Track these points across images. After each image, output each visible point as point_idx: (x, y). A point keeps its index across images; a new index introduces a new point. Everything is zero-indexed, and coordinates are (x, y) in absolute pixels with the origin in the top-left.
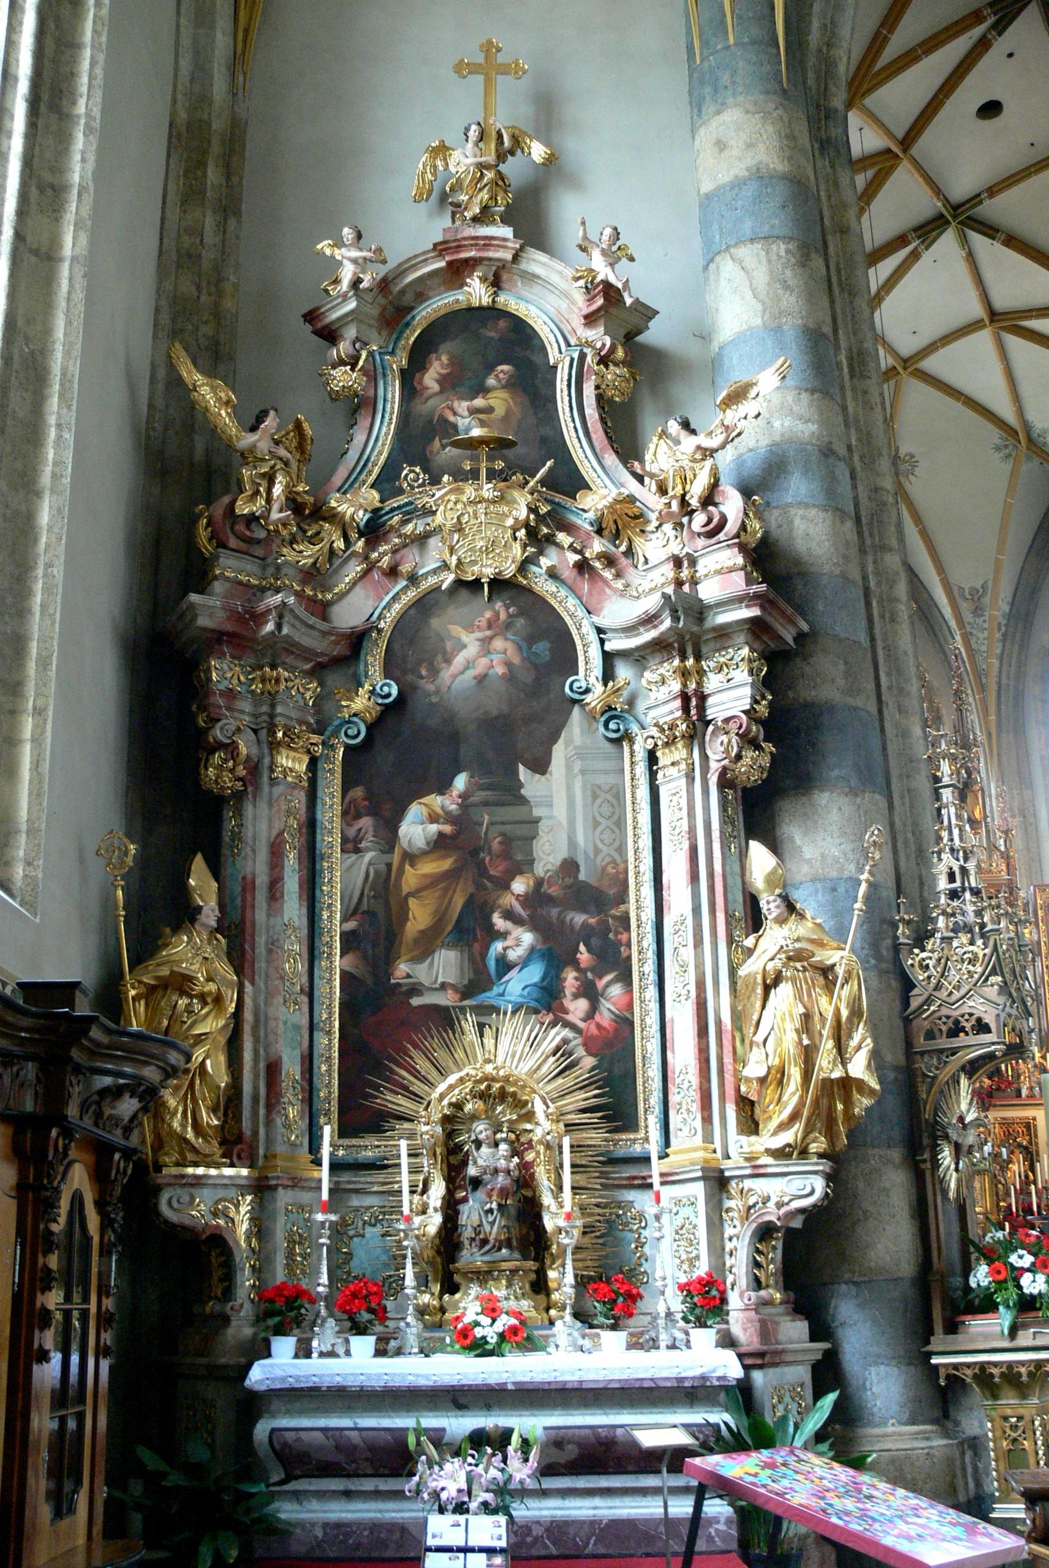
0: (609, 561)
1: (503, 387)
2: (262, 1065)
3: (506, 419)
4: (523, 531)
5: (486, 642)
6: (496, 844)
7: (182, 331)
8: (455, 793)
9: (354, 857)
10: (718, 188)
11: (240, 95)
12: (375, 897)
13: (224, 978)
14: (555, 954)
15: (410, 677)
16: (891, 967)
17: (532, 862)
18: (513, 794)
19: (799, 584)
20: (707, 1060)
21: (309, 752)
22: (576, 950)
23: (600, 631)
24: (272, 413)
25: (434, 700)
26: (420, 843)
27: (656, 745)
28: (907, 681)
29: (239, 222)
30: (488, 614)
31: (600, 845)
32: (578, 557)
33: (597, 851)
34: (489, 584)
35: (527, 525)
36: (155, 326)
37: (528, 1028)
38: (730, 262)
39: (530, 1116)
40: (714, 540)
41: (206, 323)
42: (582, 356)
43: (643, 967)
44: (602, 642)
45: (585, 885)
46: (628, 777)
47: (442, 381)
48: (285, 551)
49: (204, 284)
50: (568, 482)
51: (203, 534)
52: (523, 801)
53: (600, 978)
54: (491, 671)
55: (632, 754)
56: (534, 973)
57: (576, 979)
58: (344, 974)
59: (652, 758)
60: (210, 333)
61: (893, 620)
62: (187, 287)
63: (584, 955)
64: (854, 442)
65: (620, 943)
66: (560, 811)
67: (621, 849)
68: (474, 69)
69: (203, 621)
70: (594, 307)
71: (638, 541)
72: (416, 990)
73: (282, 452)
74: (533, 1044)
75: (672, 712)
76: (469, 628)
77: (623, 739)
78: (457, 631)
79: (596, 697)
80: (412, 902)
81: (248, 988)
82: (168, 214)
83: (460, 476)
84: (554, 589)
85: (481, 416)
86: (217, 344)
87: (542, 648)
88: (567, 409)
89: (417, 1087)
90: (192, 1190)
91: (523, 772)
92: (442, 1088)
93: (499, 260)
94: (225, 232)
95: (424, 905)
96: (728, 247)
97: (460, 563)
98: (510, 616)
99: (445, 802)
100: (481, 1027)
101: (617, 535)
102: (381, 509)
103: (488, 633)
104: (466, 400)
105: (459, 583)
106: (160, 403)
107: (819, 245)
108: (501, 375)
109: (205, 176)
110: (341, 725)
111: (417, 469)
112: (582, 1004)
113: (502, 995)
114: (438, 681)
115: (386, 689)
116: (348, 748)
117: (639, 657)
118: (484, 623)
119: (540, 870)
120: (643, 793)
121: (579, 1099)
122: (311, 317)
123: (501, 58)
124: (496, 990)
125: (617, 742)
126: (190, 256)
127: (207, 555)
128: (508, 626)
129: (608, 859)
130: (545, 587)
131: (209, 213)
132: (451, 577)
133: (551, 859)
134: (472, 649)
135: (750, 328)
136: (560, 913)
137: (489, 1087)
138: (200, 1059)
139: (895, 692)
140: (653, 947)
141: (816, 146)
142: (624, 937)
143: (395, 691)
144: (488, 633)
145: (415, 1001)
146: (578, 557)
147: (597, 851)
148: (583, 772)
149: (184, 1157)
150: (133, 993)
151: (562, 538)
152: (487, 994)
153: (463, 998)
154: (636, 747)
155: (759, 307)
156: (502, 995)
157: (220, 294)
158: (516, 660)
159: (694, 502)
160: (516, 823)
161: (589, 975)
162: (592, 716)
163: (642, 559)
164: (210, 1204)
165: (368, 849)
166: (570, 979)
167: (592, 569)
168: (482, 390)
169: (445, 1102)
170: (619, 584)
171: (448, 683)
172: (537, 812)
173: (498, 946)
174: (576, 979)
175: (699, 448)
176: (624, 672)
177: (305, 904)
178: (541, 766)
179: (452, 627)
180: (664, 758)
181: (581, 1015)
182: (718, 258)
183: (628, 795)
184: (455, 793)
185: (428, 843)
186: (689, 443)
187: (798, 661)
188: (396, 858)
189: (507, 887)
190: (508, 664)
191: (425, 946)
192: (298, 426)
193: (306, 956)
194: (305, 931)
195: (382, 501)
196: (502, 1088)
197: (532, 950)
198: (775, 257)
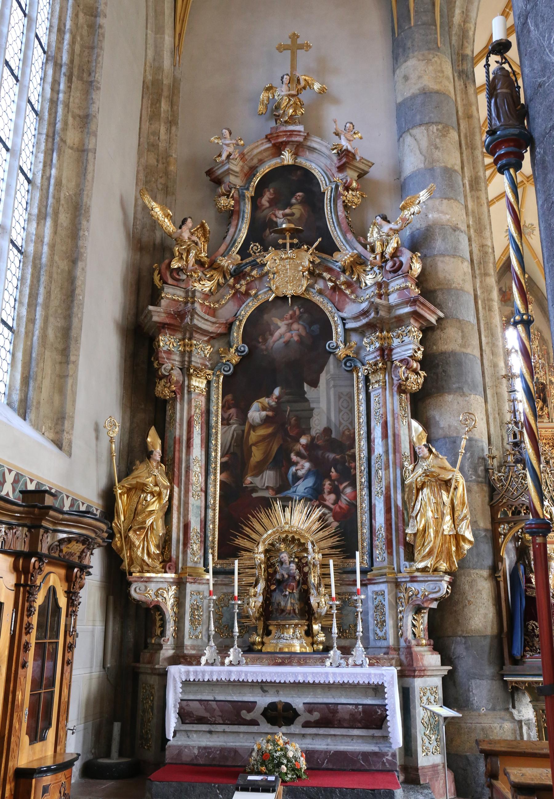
0: (349, 285)
2: (182, 525)
3: (300, 219)
5: (289, 325)
6: (293, 421)
7: (150, 181)
8: (274, 397)
9: (227, 427)
10: (404, 100)
11: (177, 65)
12: (236, 446)
13: (163, 485)
14: (320, 472)
16: (483, 480)
17: (310, 429)
18: (301, 397)
19: (439, 294)
20: (391, 525)
21: (206, 378)
22: (330, 471)
23: (343, 319)
24: (189, 220)
25: (265, 353)
26: (258, 420)
27: (369, 373)
28: (497, 340)
29: (177, 128)
30: (291, 312)
31: (342, 421)
32: (332, 284)
33: (341, 423)
35: (309, 270)
36: (137, 179)
37: (306, 508)
39: (306, 550)
40: (396, 274)
41: (161, 177)
42: (337, 187)
43: (361, 479)
44: (344, 324)
45: (335, 440)
46: (355, 389)
47: (270, 201)
48: (196, 284)
50: (329, 248)
51: (157, 278)
52: (307, 400)
53: (341, 484)
55: (358, 377)
56: (310, 482)
57: (330, 484)
58: (221, 482)
59: (367, 379)
60: (163, 182)
61: (490, 310)
62: (152, 161)
63: (333, 473)
64: (471, 223)
65: (351, 468)
66: (323, 405)
67: (352, 423)
69: (155, 318)
70: (342, 163)
72: (255, 489)
73: (195, 238)
74: (308, 516)
75: (376, 357)
76: (282, 319)
77: (353, 369)
79: (341, 352)
80: (254, 448)
81: (176, 489)
82: (143, 126)
83: (278, 247)
85: (289, 218)
86: (167, 187)
87: (316, 328)
89: (254, 536)
90: (147, 584)
91: (306, 387)
92: (265, 536)
93: (297, 142)
95: (258, 450)
96: (408, 130)
97: (277, 288)
98: (301, 313)
99: (270, 401)
100: (284, 507)
101: (352, 273)
103: (290, 321)
104: (281, 210)
105: (277, 298)
106: (139, 216)
107: (455, 125)
108: (298, 198)
109: (160, 107)
110: (222, 366)
111: (257, 244)
112: (332, 497)
113: (295, 492)
115: (242, 349)
116: (225, 376)
117: (361, 331)
118: (288, 316)
119: (313, 433)
120: (362, 396)
121: (330, 542)
122: (209, 173)
123: (299, 41)
124: (292, 490)
125: (351, 372)
126: (153, 145)
127: (159, 287)
128: (300, 318)
129: (345, 428)
130: (318, 299)
131: (162, 124)
133: (318, 428)
135: (418, 170)
136: (322, 453)
137: (287, 536)
138: (150, 523)
139: (490, 345)
140: (366, 470)
141: (456, 75)
142: (353, 465)
143: (247, 349)
144: (290, 321)
145: (254, 495)
146: (332, 284)
147: (341, 423)
148: (334, 386)
149: (142, 569)
150: (120, 491)
151: (326, 275)
152: (288, 492)
153: (276, 494)
154: (360, 374)
155: (423, 158)
156: (295, 492)
157: (168, 164)
158: (304, 334)
159: (387, 256)
160: (302, 410)
161: (336, 483)
162: (338, 360)
163: (364, 284)
164: (155, 591)
165: (233, 424)
166: (327, 484)
167: (340, 290)
168: (289, 205)
169: (267, 543)
171: (271, 344)
172: (312, 405)
173: (293, 469)
174: (330, 484)
175: (391, 229)
176: (354, 338)
177: (204, 449)
178: (314, 384)
179: (273, 319)
180: (373, 379)
181: (332, 501)
182: (404, 135)
183: (356, 397)
184: (274, 397)
185: (261, 421)
186: (386, 228)
187: (438, 332)
188: (247, 427)
189: (298, 441)
190: (300, 336)
191: (259, 470)
192: (202, 226)
193: (204, 474)
194: (204, 462)
195: (242, 260)
196: (293, 537)
197: (309, 471)
198: (431, 133)
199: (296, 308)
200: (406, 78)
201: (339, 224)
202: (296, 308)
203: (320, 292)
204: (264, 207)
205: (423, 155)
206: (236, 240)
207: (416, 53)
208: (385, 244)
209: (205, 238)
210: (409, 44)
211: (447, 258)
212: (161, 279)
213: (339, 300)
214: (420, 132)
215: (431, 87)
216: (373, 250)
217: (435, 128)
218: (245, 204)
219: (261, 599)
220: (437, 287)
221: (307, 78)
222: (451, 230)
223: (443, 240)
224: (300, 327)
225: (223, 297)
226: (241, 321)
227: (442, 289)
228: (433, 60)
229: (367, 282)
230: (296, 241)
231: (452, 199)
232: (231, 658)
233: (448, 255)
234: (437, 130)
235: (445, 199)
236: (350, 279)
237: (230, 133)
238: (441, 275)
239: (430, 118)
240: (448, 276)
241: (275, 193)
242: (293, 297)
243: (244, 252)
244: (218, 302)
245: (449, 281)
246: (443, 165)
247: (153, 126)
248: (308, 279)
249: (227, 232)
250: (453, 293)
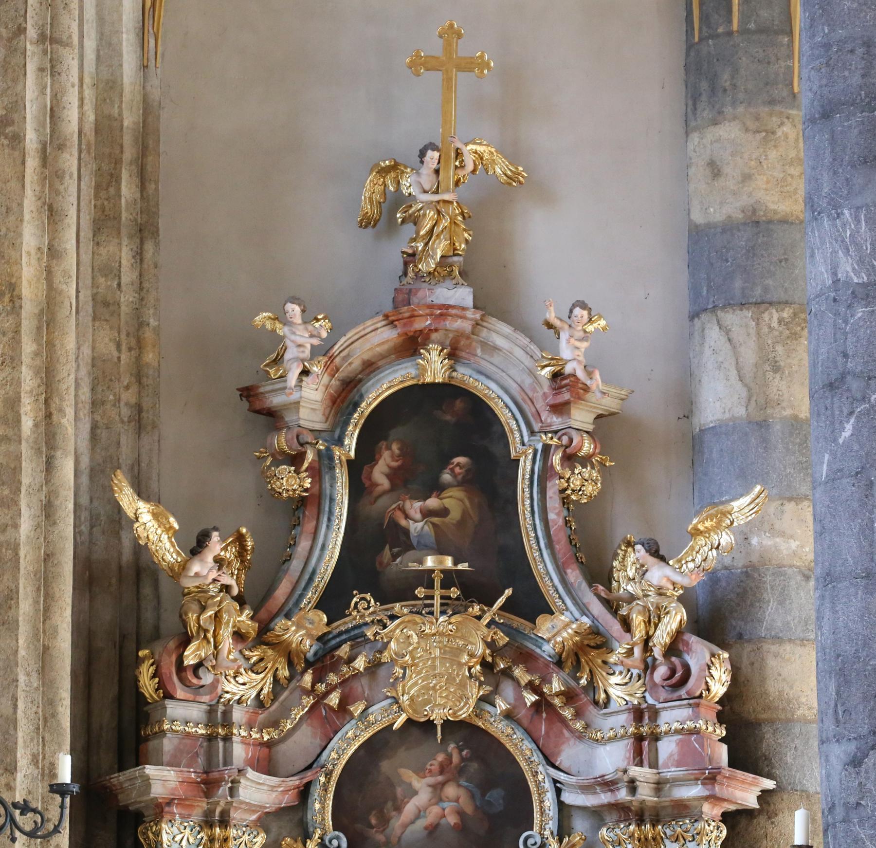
1: (460, 484)
3: (461, 523)
4: (478, 667)
5: (437, 788)
7: (103, 403)
10: (709, 226)
11: (152, 64)
15: (359, 826)
24: (215, 536)
29: (157, 244)
30: (441, 757)
34: (442, 725)
35: (484, 663)
38: (716, 328)
40: (675, 695)
41: (127, 388)
44: (558, 792)
47: (393, 475)
49: (123, 336)
54: (443, 821)
60: (133, 401)
62: (107, 348)
68: (429, 64)
71: (600, 673)
76: (421, 772)
78: (408, 775)
84: (509, 731)
85: (435, 520)
87: (496, 795)
88: (528, 515)
94: (141, 260)
98: (463, 759)
102: (329, 633)
103: (440, 778)
105: (409, 721)
106: (84, 500)
108: (457, 470)
111: (368, 596)
114: (388, 831)
118: (435, 767)
122: (248, 393)
126: (106, 304)
128: (461, 771)
130: (500, 729)
131: (125, 241)
132: (403, 718)
134: (423, 796)
135: (733, 419)
144: (440, 778)
155: (744, 393)
157: (140, 345)
158: (469, 809)
163: (603, 696)
167: (550, 706)
168: (436, 487)
170: (579, 725)
171: (398, 832)
176: (580, 826)
182: (704, 317)
186: (658, 574)
187: (762, 820)
190: (460, 813)
195: (328, 624)
198: (766, 330)
199: (452, 746)
200: (715, 170)
201: (550, 545)
202: (452, 746)
203: (508, 716)
204: (379, 489)
205: (746, 385)
206: (314, 573)
207: (741, 109)
208: (654, 619)
209: (242, 562)
210: (725, 79)
211: (788, 647)
212: (161, 686)
213: (547, 733)
215: (772, 207)
216: (626, 624)
217: (776, 316)
218: (333, 478)
220: (764, 716)
221: (480, 149)
222: (799, 578)
224: (462, 794)
225: (285, 712)
226: (329, 775)
227: (772, 722)
228: (779, 133)
229: (611, 691)
230: (454, 592)
233: (790, 640)
234: (780, 322)
235: (790, 499)
236: (573, 683)
237: (303, 311)
238: (773, 687)
239: (766, 289)
240: (787, 689)
241: (403, 454)
242: (446, 723)
243: (333, 602)
244: (275, 724)
245: (789, 701)
246: (788, 412)
247: (103, 251)
248: (481, 684)
250: (797, 730)
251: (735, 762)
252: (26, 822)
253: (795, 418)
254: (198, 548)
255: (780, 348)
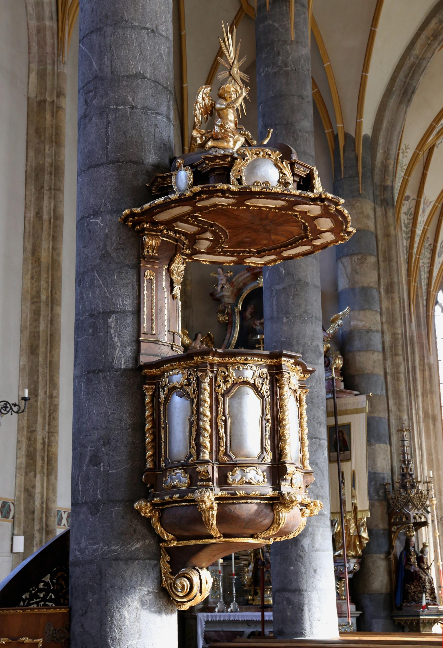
24: (199, 335)
28: (402, 400)
47: (252, 314)
61: (398, 380)
64: (384, 320)
139: (398, 404)
155: (348, 280)
192: (209, 335)
205: (348, 278)
206: (230, 343)
211: (362, 353)
214: (346, 260)
217: (356, 258)
218: (235, 316)
219: (251, 574)
223: (360, 340)
228: (356, 205)
231: (367, 309)
232: (232, 608)
233: (363, 351)
234: (358, 259)
235: (362, 310)
246: (361, 285)
249: (225, 336)
251: (346, 387)
252: (15, 409)
253: (363, 286)
254: (195, 339)
255: (358, 267)
